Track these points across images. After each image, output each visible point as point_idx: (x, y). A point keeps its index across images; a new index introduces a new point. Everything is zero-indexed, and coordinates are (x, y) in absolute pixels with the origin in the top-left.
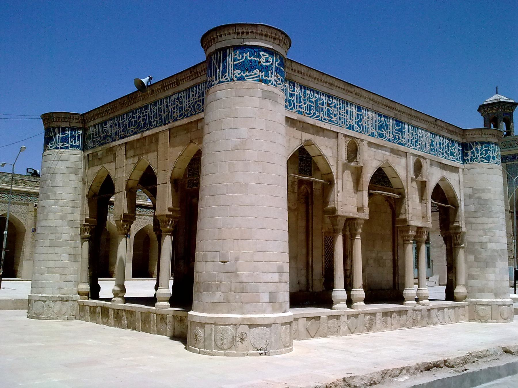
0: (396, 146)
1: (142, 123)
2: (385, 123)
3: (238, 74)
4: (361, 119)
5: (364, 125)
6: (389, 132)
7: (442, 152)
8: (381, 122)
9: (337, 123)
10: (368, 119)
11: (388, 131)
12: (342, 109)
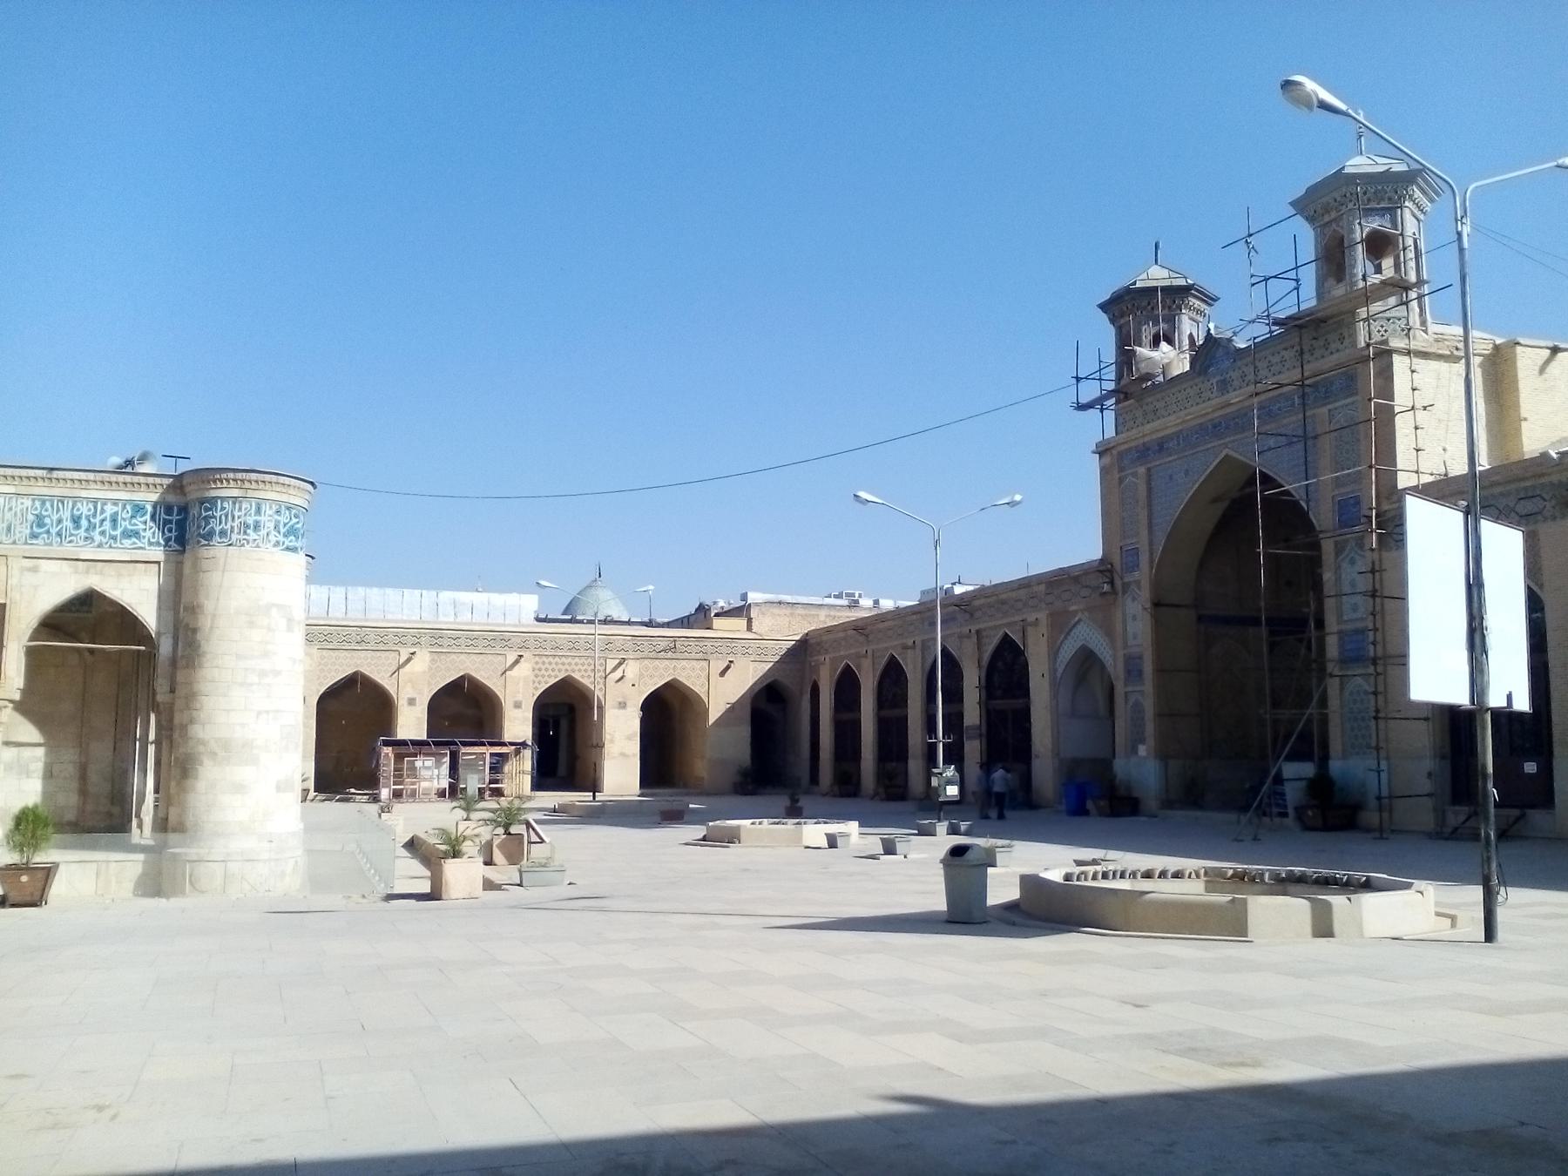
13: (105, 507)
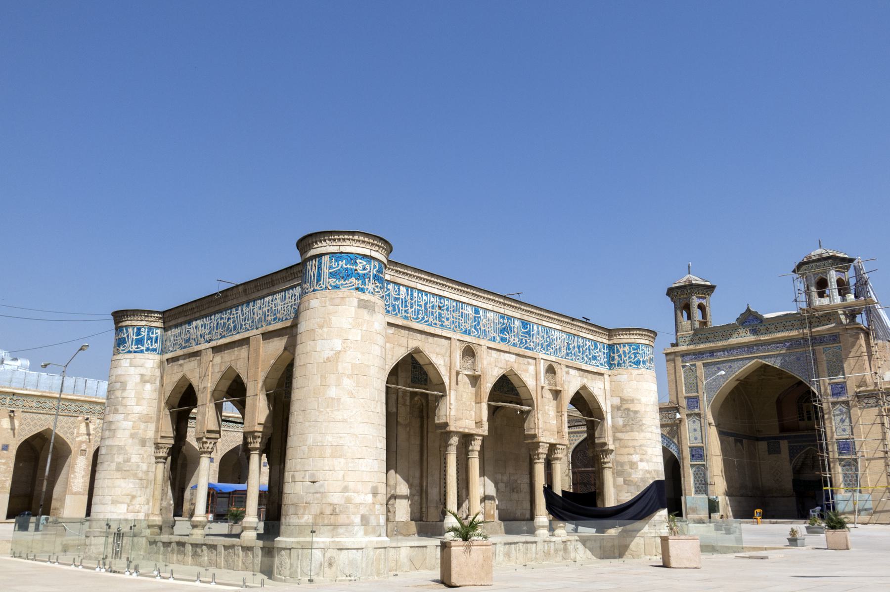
0: (522, 351)
1: (232, 325)
3: (333, 283)
4: (479, 323)
5: (483, 328)
8: (503, 324)
9: (450, 328)
10: (488, 322)
11: (513, 334)
12: (456, 311)
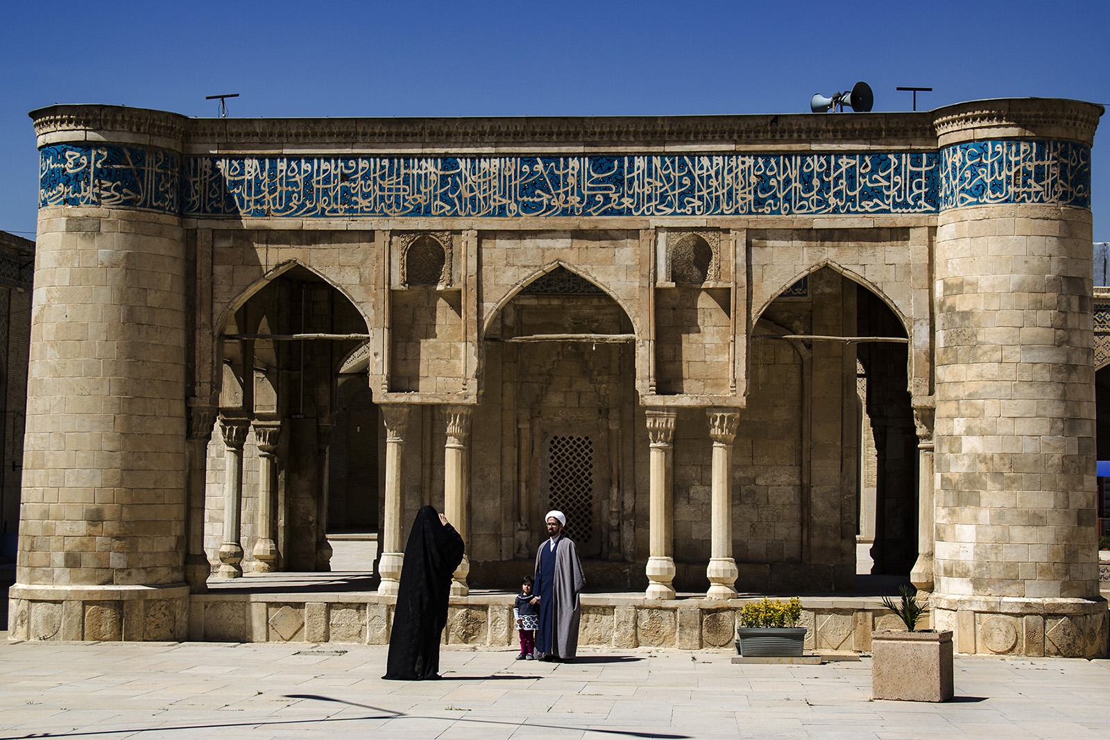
2: (551, 172)
4: (455, 187)
6: (566, 193)
7: (815, 197)
8: (532, 173)
9: (373, 211)
10: (482, 180)
13: (840, 162)
